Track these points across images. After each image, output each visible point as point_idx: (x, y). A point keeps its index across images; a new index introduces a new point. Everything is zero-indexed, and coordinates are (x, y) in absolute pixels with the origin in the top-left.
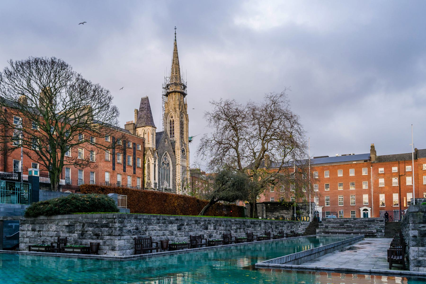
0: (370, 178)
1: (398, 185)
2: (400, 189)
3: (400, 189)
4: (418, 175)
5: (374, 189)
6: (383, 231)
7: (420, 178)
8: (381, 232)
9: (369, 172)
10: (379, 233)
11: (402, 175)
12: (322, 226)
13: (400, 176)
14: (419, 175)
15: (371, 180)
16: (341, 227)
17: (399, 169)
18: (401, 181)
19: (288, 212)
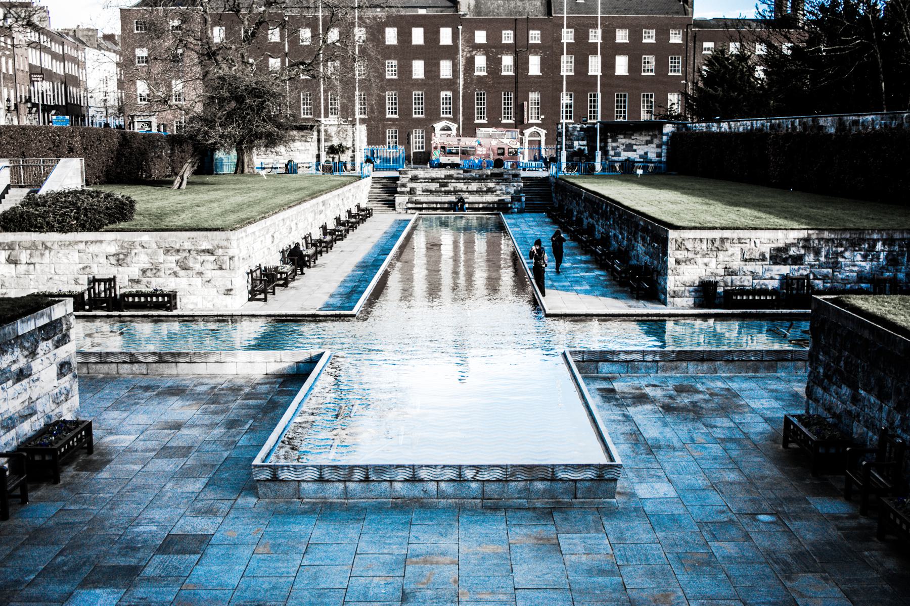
1: (512, 73)
2: (516, 82)
3: (516, 82)
6: (523, 199)
8: (519, 200)
9: (455, 36)
10: (516, 203)
12: (403, 189)
16: (443, 189)
17: (515, 36)
19: (305, 146)
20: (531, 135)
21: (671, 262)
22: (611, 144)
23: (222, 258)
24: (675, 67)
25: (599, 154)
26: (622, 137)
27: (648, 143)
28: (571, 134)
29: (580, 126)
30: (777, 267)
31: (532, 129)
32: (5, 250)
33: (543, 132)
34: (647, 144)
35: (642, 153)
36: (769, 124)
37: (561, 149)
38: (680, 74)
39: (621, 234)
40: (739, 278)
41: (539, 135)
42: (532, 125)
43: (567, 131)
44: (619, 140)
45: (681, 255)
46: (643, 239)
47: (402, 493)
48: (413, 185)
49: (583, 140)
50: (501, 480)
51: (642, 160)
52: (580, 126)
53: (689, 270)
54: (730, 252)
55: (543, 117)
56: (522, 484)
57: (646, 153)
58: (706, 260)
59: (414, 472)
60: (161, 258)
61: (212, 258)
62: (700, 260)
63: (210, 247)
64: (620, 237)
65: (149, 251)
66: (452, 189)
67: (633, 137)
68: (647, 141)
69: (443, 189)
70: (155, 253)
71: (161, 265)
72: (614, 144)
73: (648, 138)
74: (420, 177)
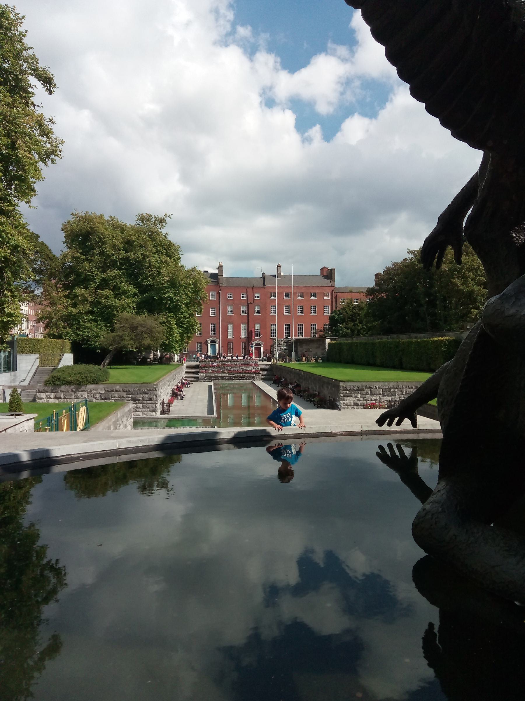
11: (250, 303)
20: (255, 345)
22: (299, 349)
25: (293, 353)
27: (317, 348)
30: (385, 397)
31: (256, 342)
32: (54, 392)
33: (262, 343)
35: (315, 352)
43: (278, 342)
45: (345, 392)
46: (328, 387)
57: (317, 353)
64: (315, 388)
72: (301, 349)
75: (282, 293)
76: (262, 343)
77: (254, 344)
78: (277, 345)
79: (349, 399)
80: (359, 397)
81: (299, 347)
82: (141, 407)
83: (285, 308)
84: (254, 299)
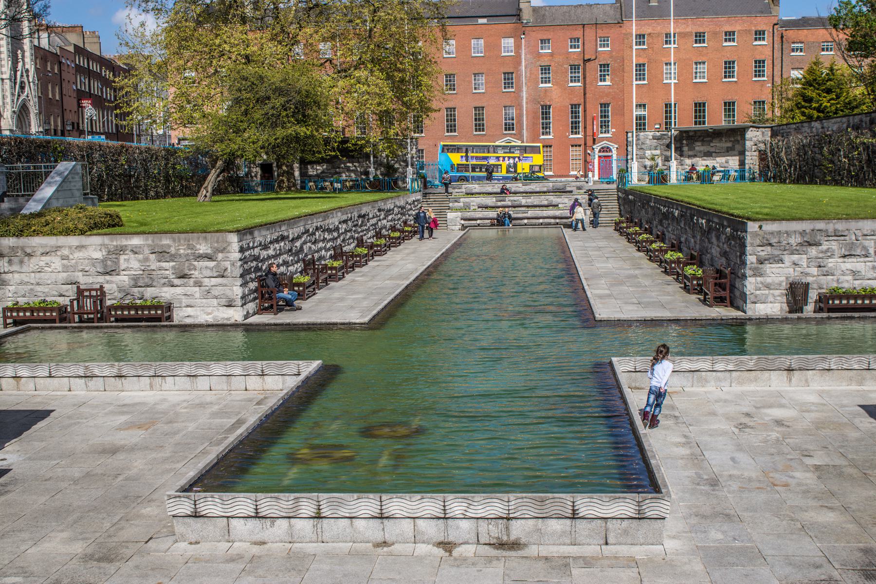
0: (520, 63)
1: (579, 84)
2: (585, 94)
3: (585, 94)
4: (623, 61)
5: (527, 92)
7: (626, 68)
9: (518, 47)
11: (589, 60)
12: (456, 204)
13: (586, 61)
14: (626, 61)
15: (521, 70)
18: (588, 75)
20: (600, 151)
21: (751, 259)
23: (223, 263)
24: (759, 71)
26: (699, 144)
28: (643, 143)
29: (652, 134)
33: (614, 147)
34: (728, 152)
36: (868, 118)
37: (632, 159)
38: (765, 79)
39: (694, 237)
40: (835, 278)
41: (611, 151)
42: (603, 139)
43: (638, 140)
44: (697, 148)
47: (367, 535)
48: (467, 200)
49: (656, 149)
50: (502, 518)
51: (723, 169)
52: (652, 134)
53: (773, 270)
54: (824, 247)
55: (614, 130)
56: (531, 522)
57: (727, 162)
58: (795, 257)
59: (381, 506)
60: (154, 265)
61: (212, 264)
62: (788, 259)
63: (209, 251)
65: (141, 257)
66: (510, 204)
67: (712, 144)
68: (727, 148)
69: (499, 204)
70: (146, 259)
71: (154, 273)
72: (691, 153)
73: (729, 145)
74: (474, 191)
75: (659, 35)
76: (614, 147)
77: (597, 151)
78: (634, 146)
79: (773, 270)
80: (805, 264)
81: (685, 149)
82: (197, 295)
83: (667, 69)
84: (596, 51)
